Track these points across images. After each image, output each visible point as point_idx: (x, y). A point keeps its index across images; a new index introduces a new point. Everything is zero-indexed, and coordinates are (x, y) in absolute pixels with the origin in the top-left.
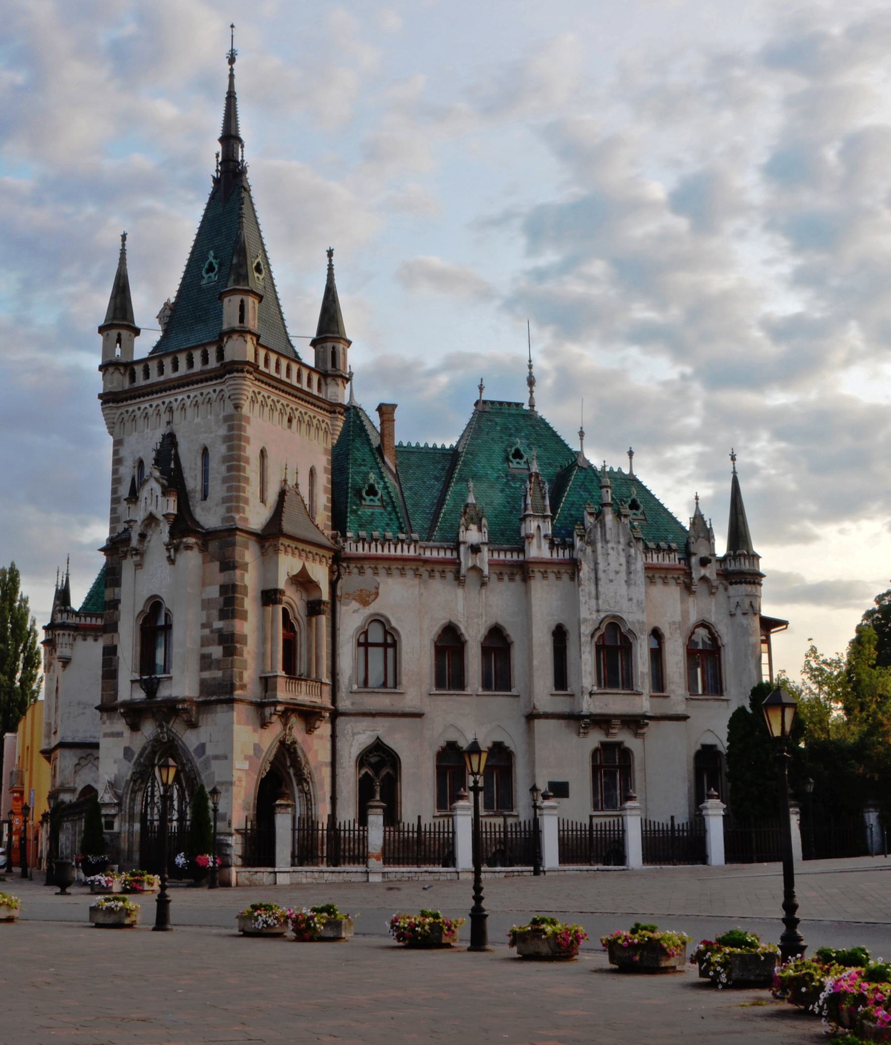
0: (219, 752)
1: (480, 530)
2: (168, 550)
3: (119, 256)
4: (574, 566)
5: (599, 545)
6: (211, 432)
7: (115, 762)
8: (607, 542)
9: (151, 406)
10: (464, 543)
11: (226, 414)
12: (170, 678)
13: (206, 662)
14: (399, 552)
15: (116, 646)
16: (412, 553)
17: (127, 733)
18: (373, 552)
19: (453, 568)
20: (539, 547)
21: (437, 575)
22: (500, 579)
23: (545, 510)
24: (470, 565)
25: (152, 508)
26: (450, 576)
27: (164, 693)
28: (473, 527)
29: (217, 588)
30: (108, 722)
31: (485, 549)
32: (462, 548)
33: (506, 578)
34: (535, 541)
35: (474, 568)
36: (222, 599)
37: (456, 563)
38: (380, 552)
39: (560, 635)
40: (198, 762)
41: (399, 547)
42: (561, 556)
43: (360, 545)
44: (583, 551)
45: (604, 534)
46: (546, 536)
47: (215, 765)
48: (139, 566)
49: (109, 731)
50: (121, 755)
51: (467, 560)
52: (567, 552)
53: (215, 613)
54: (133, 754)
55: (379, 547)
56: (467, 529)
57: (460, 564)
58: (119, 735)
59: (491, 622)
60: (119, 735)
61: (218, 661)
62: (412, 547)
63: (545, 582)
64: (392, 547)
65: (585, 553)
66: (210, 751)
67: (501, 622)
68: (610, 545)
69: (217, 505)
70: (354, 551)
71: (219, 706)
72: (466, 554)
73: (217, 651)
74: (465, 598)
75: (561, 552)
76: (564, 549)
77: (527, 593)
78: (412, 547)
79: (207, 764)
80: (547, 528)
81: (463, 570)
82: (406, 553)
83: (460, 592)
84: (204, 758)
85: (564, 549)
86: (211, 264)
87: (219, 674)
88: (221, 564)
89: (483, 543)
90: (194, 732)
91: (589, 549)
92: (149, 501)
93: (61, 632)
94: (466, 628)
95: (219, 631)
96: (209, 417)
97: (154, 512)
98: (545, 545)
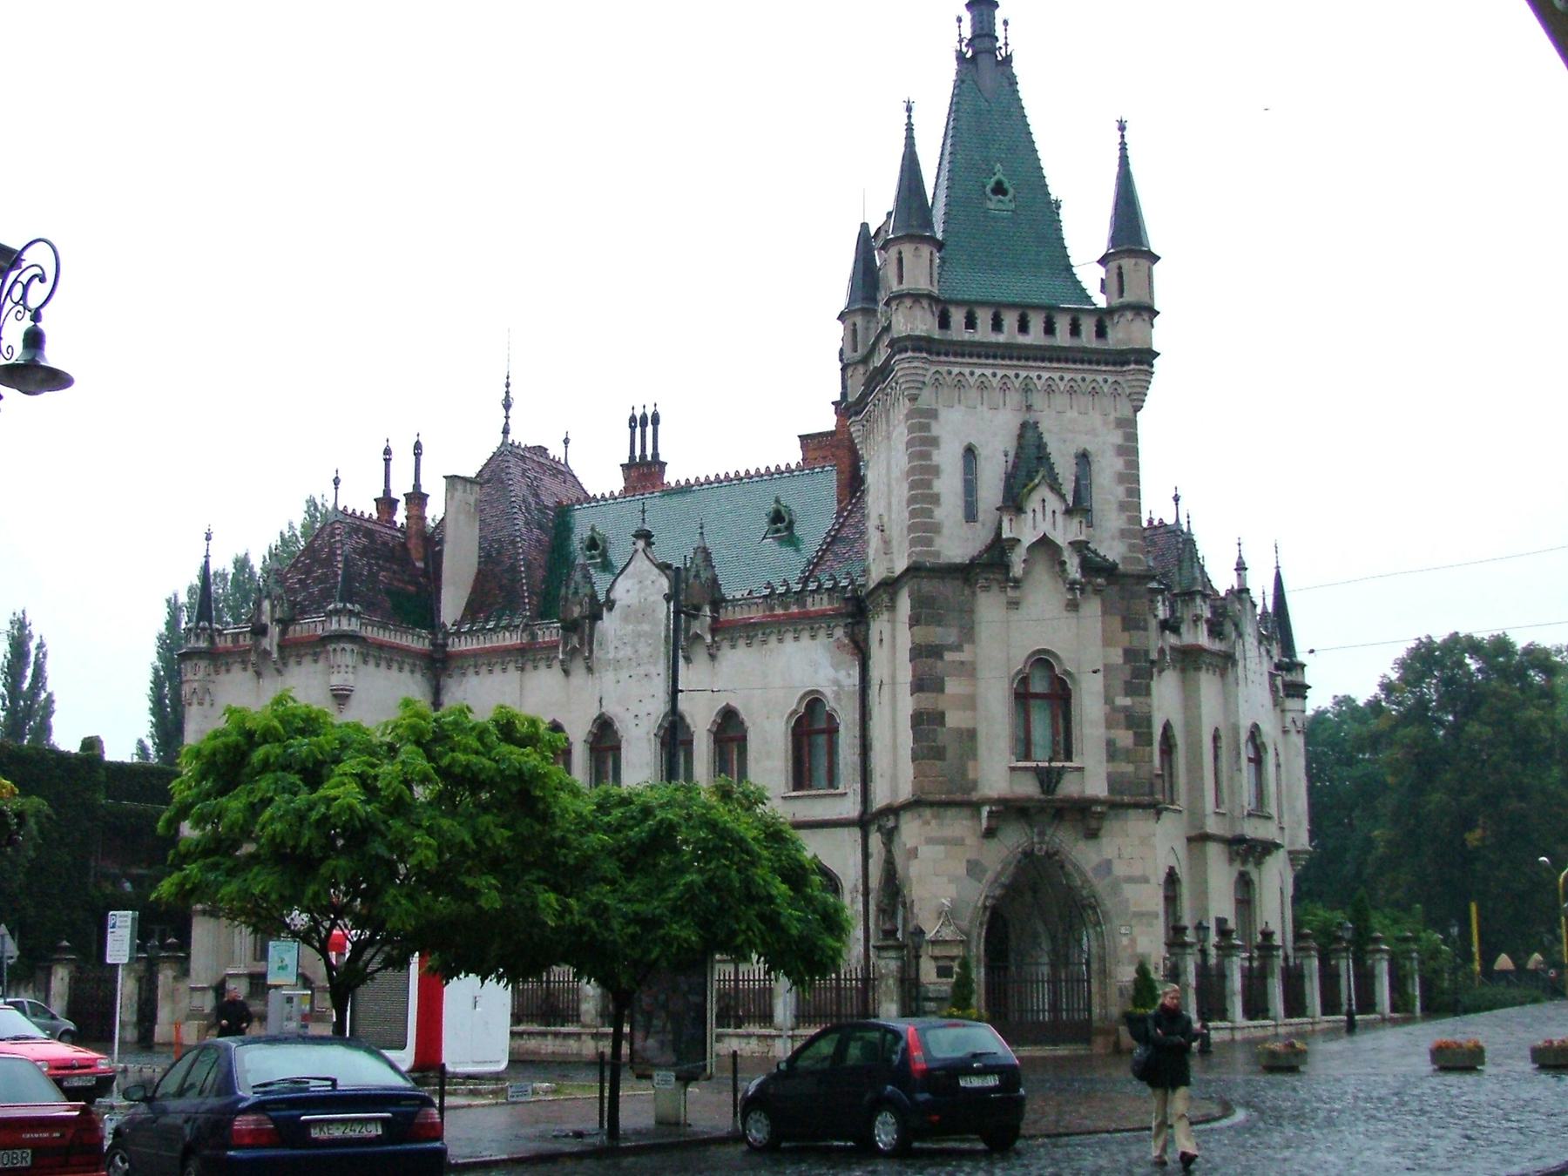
0: (1137, 871)
2: (1071, 589)
3: (904, 134)
6: (1096, 436)
7: (950, 881)
9: (994, 375)
11: (1118, 415)
12: (1080, 769)
13: (1112, 752)
15: (942, 715)
17: (971, 840)
25: (1044, 527)
27: (1069, 788)
29: (1120, 652)
30: (933, 822)
36: (1128, 669)
39: (1216, 738)
40: (1101, 886)
47: (1129, 891)
48: (1014, 604)
49: (934, 834)
50: (962, 870)
53: (1118, 684)
54: (984, 871)
58: (959, 842)
60: (959, 842)
61: (1127, 751)
66: (1120, 869)
69: (1113, 538)
71: (1131, 812)
73: (1125, 738)
79: (1115, 887)
84: (1107, 880)
86: (999, 184)
87: (1130, 768)
88: (1124, 619)
90: (1091, 843)
92: (1039, 516)
93: (348, 646)
95: (1125, 709)
96: (1091, 412)
97: (1052, 535)
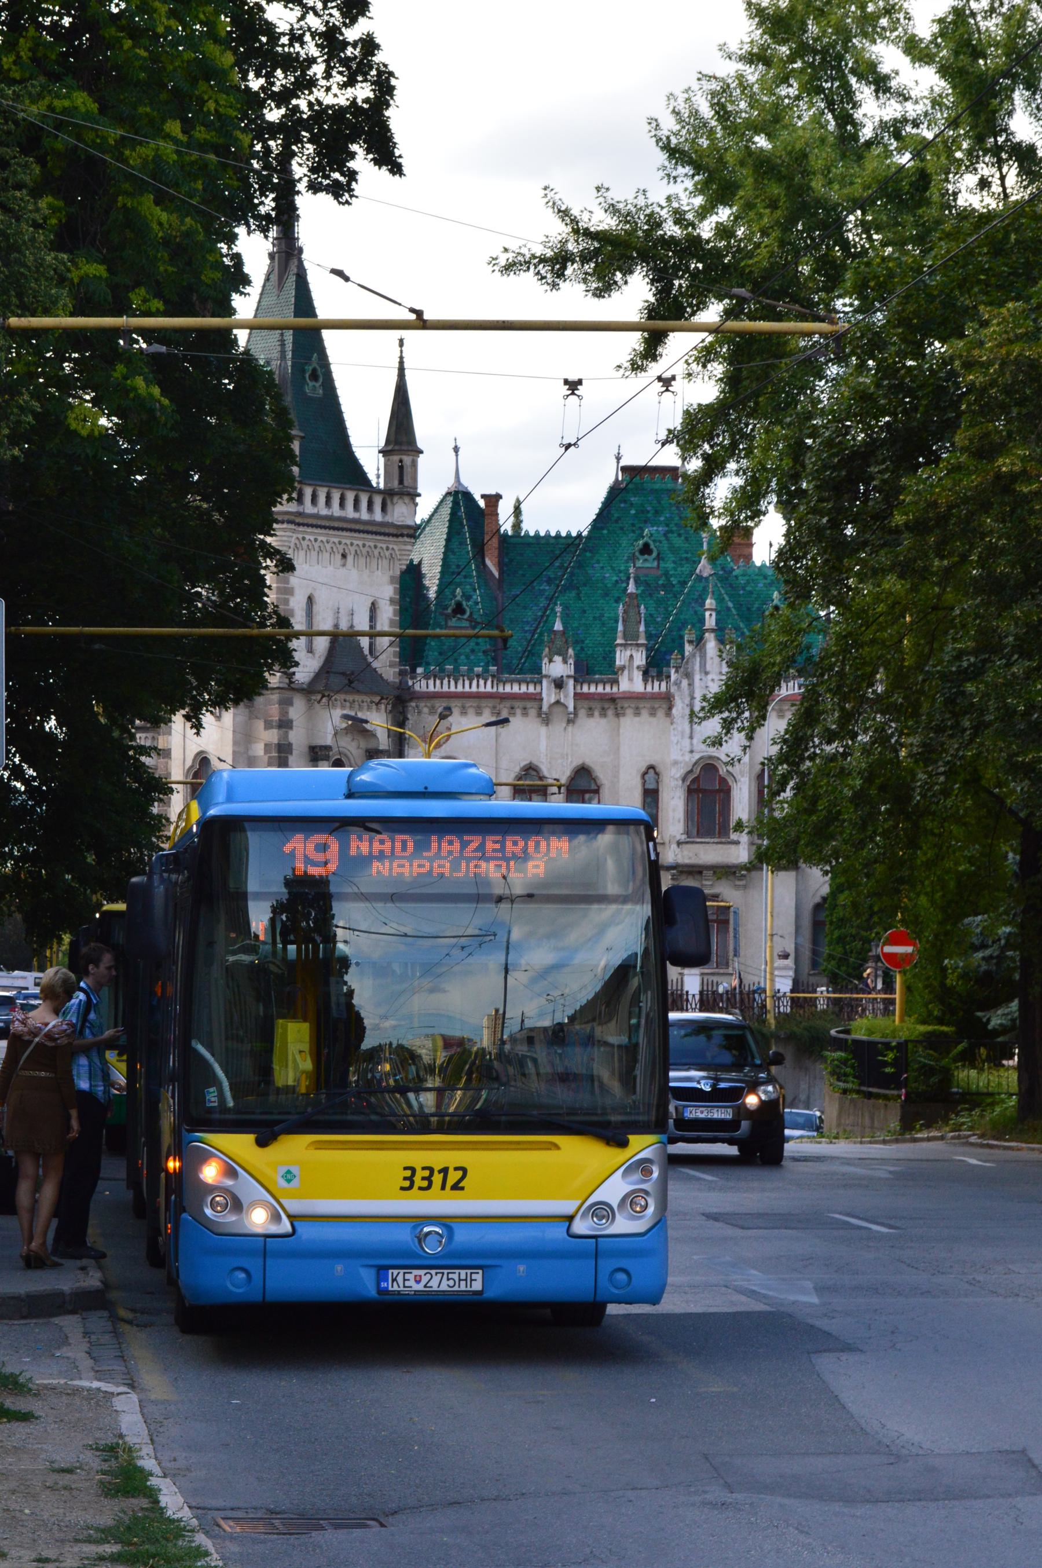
1: (565, 661)
4: (667, 700)
5: (697, 677)
8: (707, 673)
10: (546, 676)
14: (474, 689)
16: (489, 689)
18: (445, 689)
19: (535, 704)
20: (631, 679)
21: (518, 711)
22: (590, 715)
23: (637, 638)
24: (553, 701)
26: (533, 712)
28: (558, 659)
31: (571, 682)
32: (545, 682)
33: (596, 713)
34: (626, 672)
35: (558, 702)
37: (537, 698)
38: (453, 689)
41: (475, 682)
42: (656, 689)
43: (431, 682)
44: (678, 684)
45: (703, 665)
46: (638, 667)
51: (549, 695)
52: (664, 684)
55: (452, 683)
56: (550, 661)
57: (542, 700)
59: (577, 762)
62: (489, 683)
63: (637, 719)
64: (467, 683)
65: (679, 687)
67: (589, 762)
68: (710, 677)
70: (424, 689)
72: (549, 689)
74: (548, 737)
75: (656, 684)
76: (660, 681)
77: (616, 731)
78: (489, 683)
80: (640, 658)
81: (545, 708)
82: (482, 689)
83: (543, 730)
85: (660, 681)
89: (569, 677)
91: (685, 683)
94: (549, 770)
98: (638, 676)
